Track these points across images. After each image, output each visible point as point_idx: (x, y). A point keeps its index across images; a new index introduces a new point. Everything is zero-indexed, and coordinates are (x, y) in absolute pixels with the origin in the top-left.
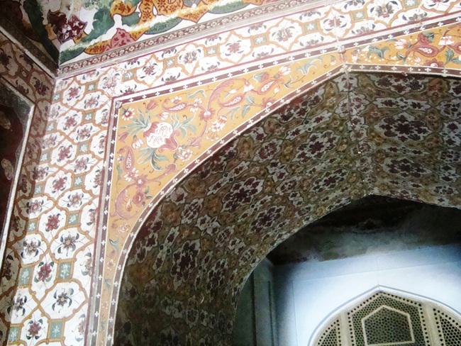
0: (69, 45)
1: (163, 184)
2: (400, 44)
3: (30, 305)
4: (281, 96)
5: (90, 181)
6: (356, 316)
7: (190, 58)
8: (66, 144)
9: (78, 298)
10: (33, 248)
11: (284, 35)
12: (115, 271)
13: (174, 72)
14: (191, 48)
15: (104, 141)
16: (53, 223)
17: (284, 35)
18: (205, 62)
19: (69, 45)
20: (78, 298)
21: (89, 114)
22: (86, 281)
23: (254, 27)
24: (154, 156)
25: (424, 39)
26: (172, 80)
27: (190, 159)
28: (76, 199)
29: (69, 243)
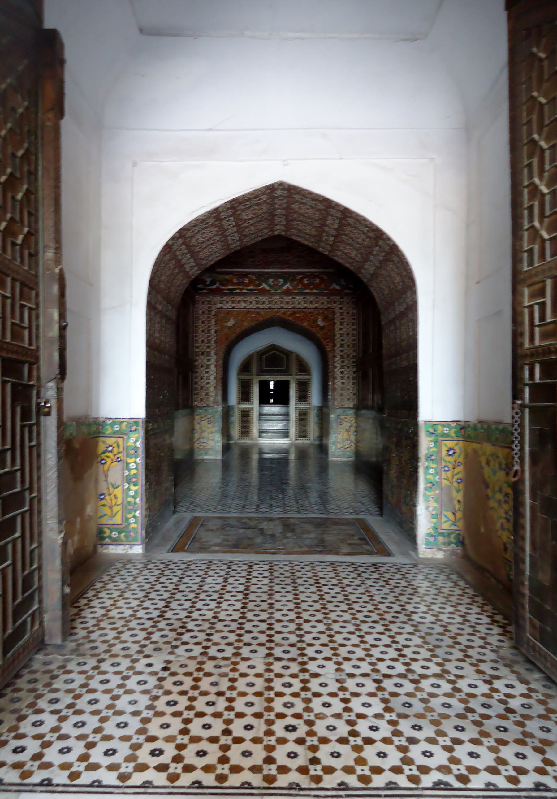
0: (200, 286)
1: (232, 337)
2: (289, 312)
3: (200, 361)
4: (261, 319)
5: (213, 331)
6: (261, 354)
7: (239, 302)
8: (204, 319)
9: (213, 361)
10: (198, 347)
11: (263, 303)
12: (221, 354)
13: (234, 305)
14: (239, 299)
15: (216, 321)
16: (203, 341)
17: (263, 303)
18: (244, 305)
19: (200, 286)
20: (213, 361)
21: (210, 312)
22: (215, 357)
23: (257, 298)
24: (230, 328)
25: (294, 313)
26: (233, 308)
27: (238, 331)
28: (209, 336)
29: (209, 347)
